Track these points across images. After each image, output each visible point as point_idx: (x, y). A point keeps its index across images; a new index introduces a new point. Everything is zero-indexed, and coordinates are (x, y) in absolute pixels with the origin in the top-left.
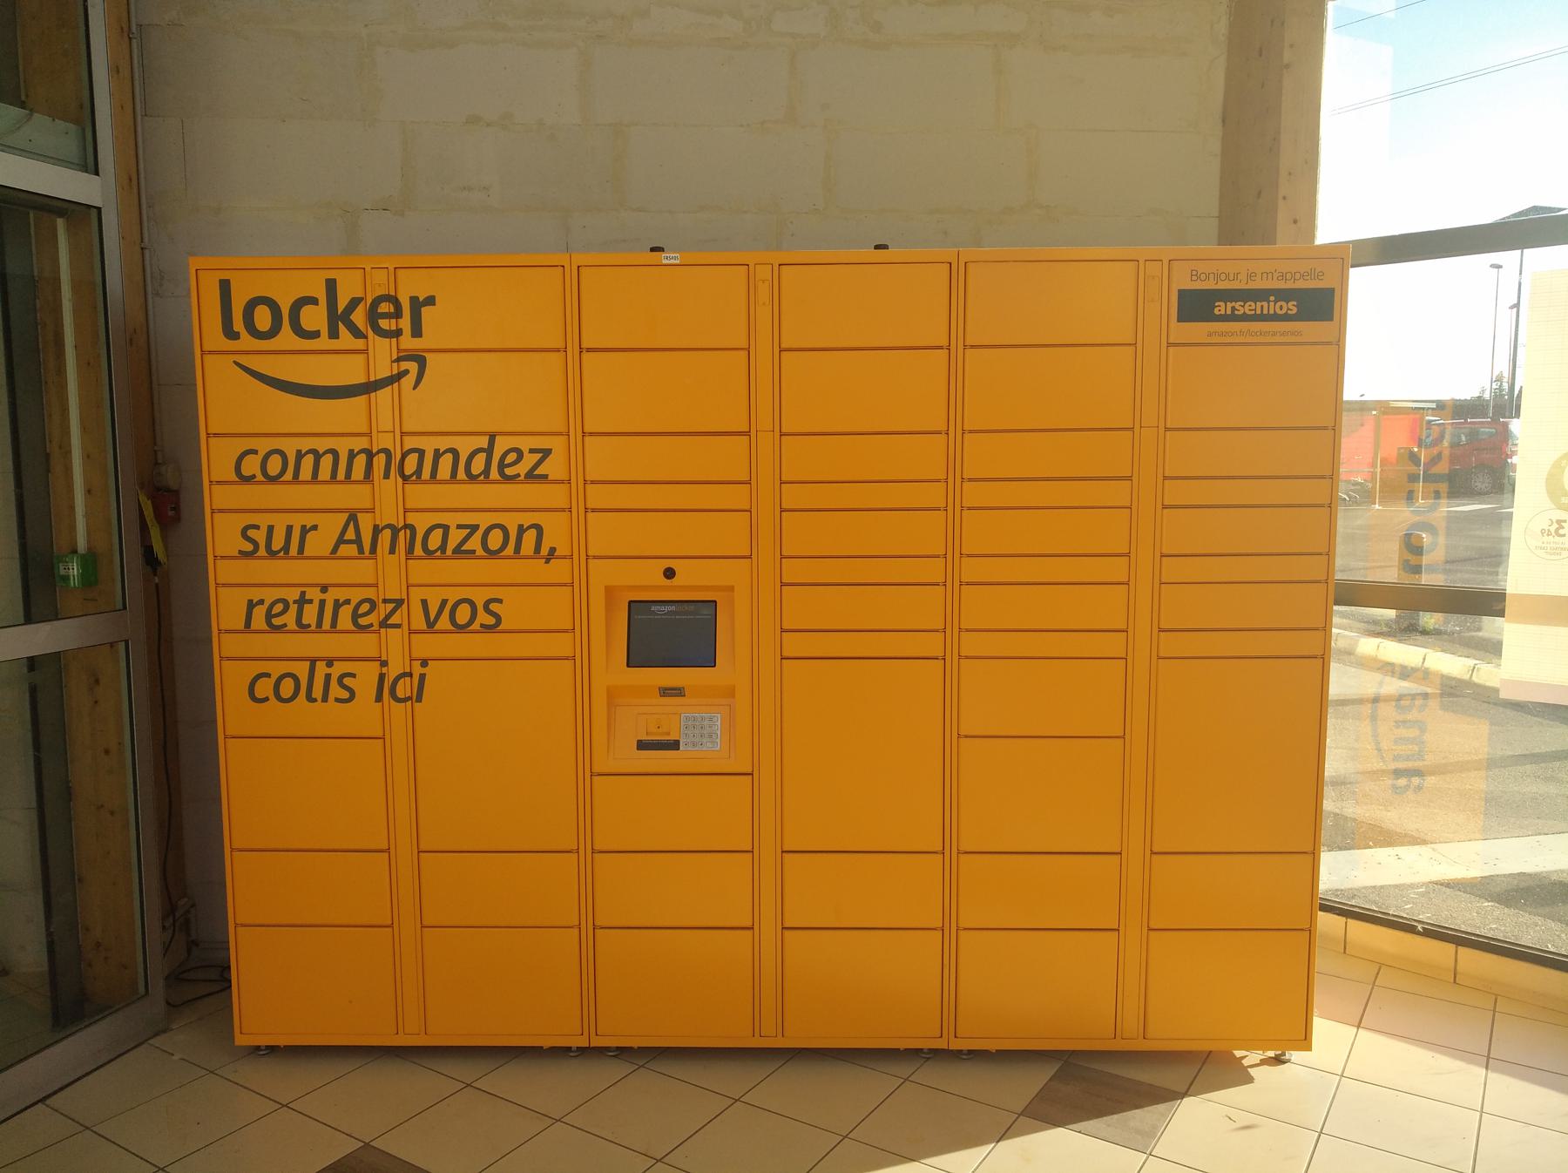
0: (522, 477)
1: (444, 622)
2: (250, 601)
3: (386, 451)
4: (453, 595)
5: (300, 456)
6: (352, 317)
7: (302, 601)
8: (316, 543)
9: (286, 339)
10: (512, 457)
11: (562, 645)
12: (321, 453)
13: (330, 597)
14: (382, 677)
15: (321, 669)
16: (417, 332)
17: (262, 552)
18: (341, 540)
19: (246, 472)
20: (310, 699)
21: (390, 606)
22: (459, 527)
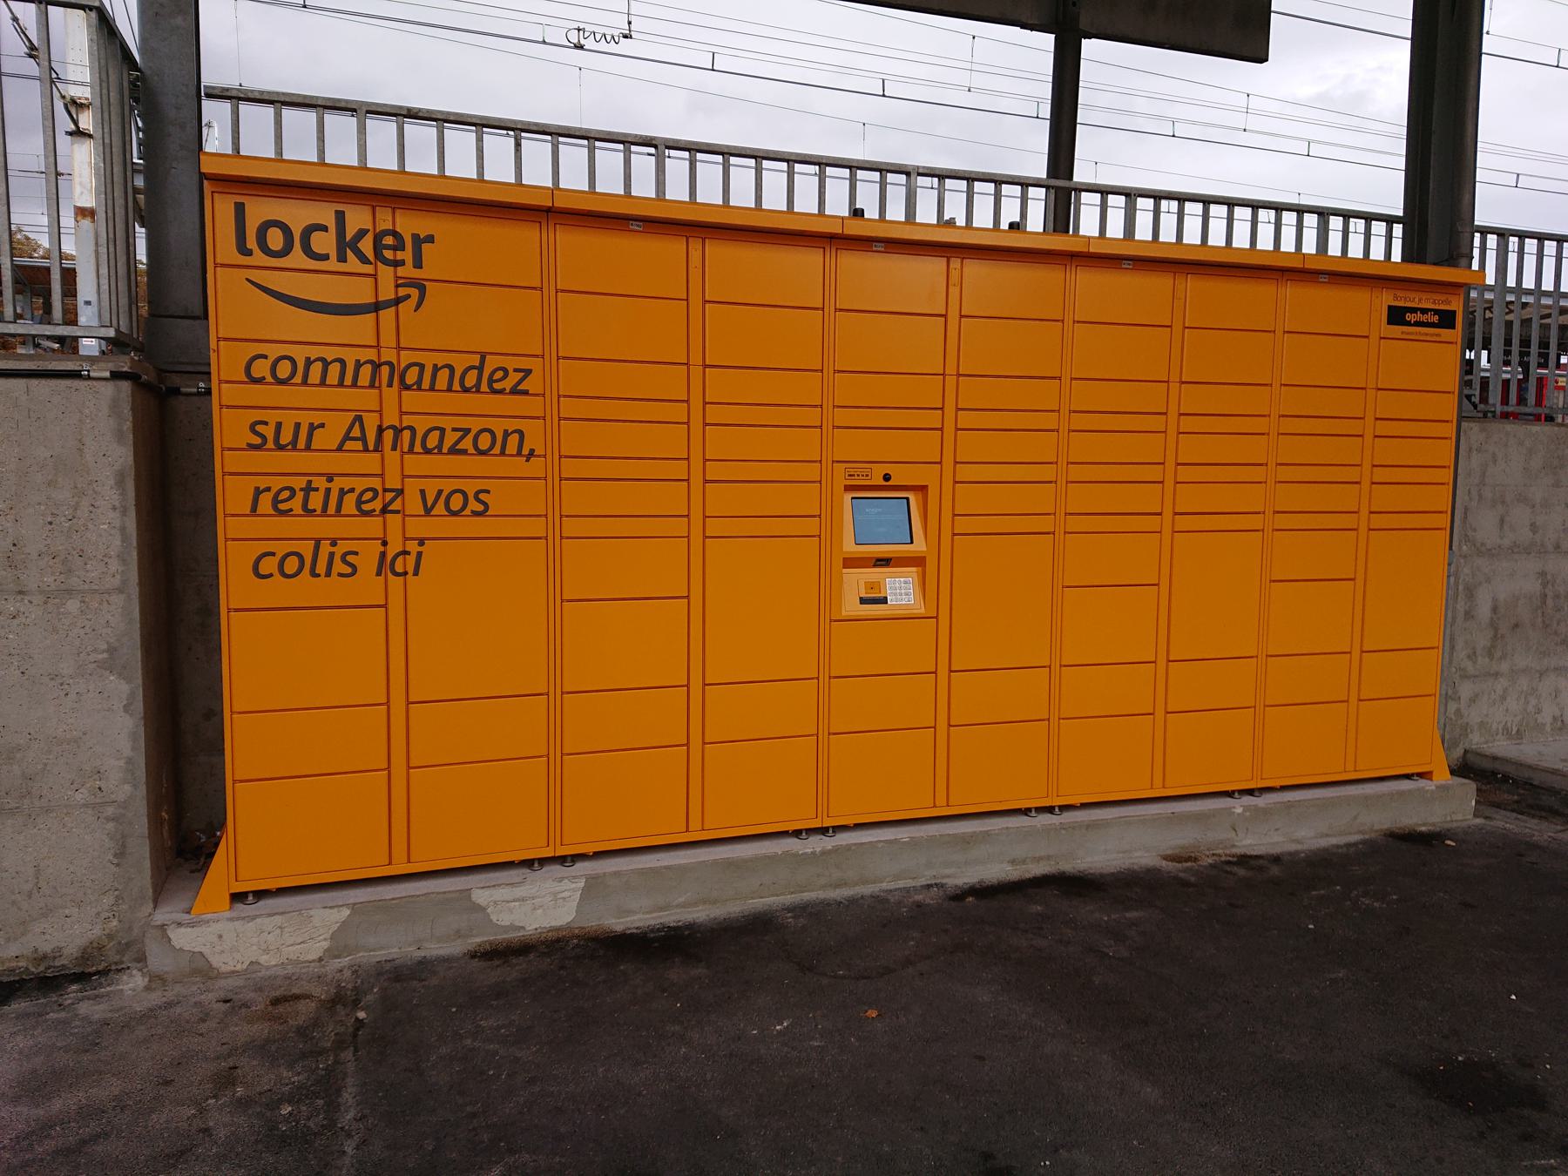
0: (508, 391)
1: (440, 509)
2: (257, 489)
3: (390, 364)
4: (449, 484)
5: (309, 362)
7: (309, 489)
8: (319, 439)
9: (297, 258)
10: (500, 374)
14: (383, 555)
15: (325, 548)
16: (418, 264)
17: (270, 445)
18: (347, 437)
19: (256, 374)
20: (314, 574)
21: (389, 496)
22: (454, 430)
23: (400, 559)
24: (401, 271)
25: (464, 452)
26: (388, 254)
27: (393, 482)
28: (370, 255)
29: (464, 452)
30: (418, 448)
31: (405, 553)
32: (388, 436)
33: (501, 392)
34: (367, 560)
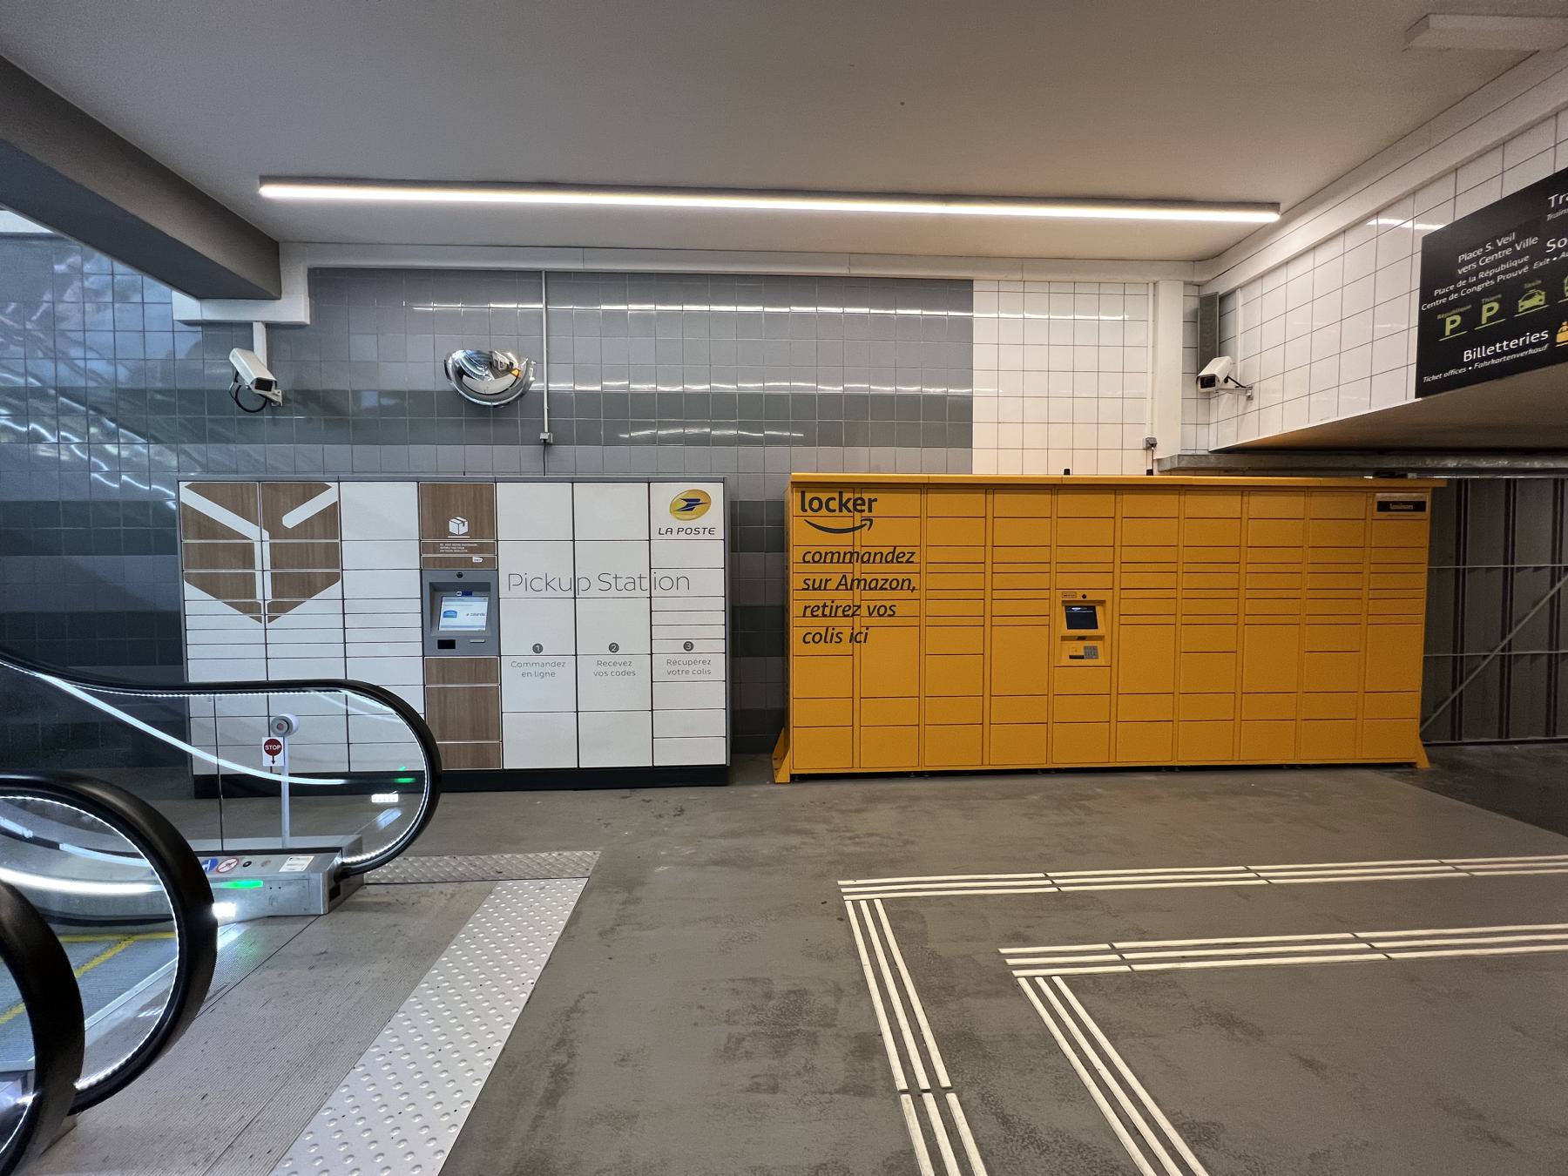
1: (875, 613)
4: (879, 604)
7: (825, 606)
9: (824, 511)
13: (834, 605)
14: (852, 633)
16: (870, 511)
17: (811, 588)
18: (840, 584)
20: (826, 642)
21: (855, 608)
23: (858, 636)
24: (864, 514)
25: (886, 589)
26: (859, 507)
27: (857, 603)
28: (852, 509)
29: (886, 589)
30: (867, 588)
31: (861, 633)
33: (902, 562)
34: (846, 636)
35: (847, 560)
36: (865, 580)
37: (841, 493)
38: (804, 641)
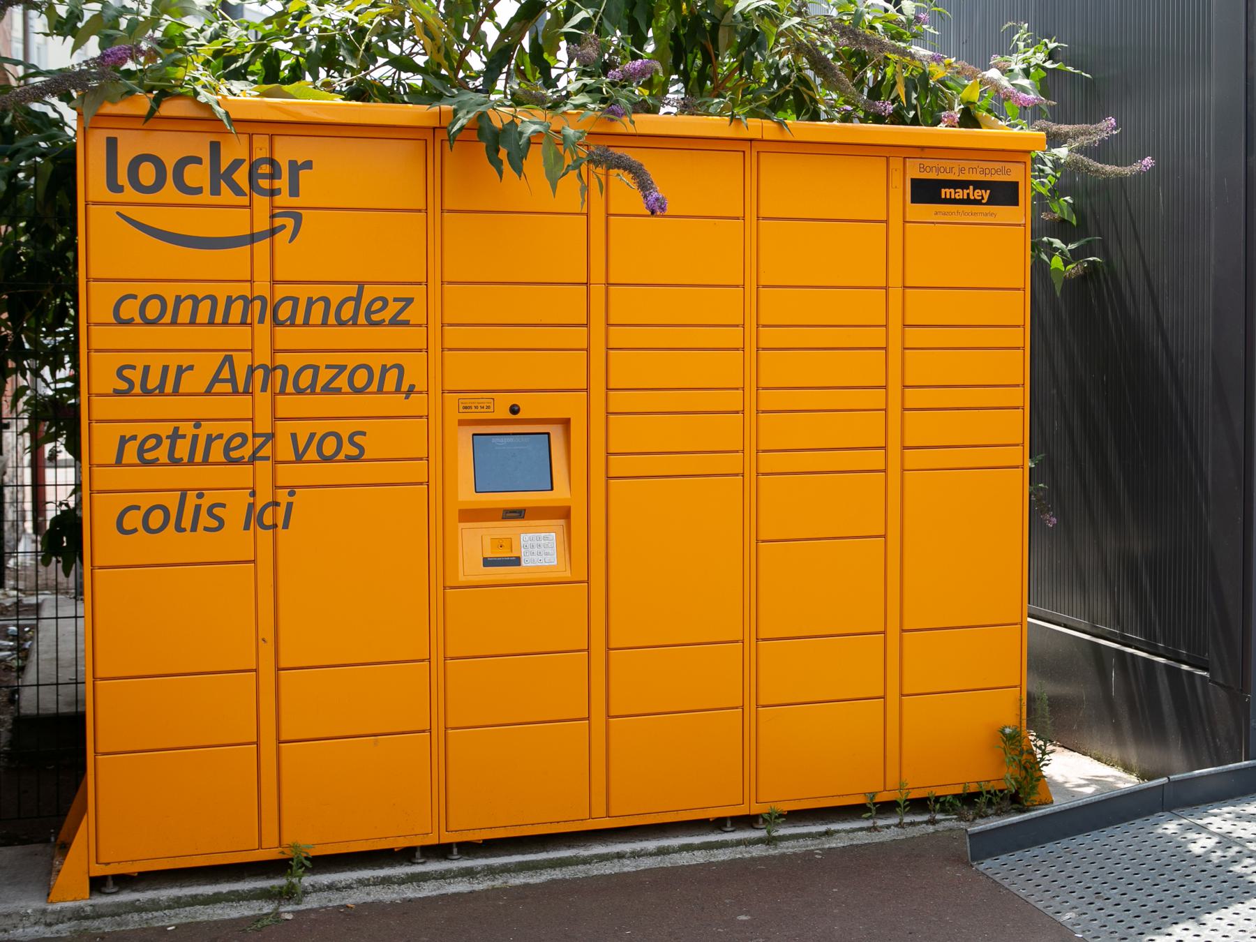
0: (387, 322)
1: (312, 454)
2: (123, 437)
3: (262, 299)
4: (321, 428)
5: (179, 301)
6: (234, 176)
7: (175, 436)
8: (187, 383)
9: (169, 192)
10: (378, 305)
11: (417, 471)
12: (200, 298)
13: (203, 434)
14: (251, 506)
15: (192, 499)
16: (294, 191)
17: (137, 389)
18: (216, 379)
19: (124, 315)
20: (179, 529)
21: (259, 441)
22: (328, 367)
23: (270, 509)
25: (338, 391)
27: (264, 426)
28: (244, 184)
29: (338, 391)
30: (290, 388)
32: (259, 374)
34: (235, 514)
35: (235, 315)
36: (285, 369)
37: (215, 148)
38: (122, 530)
